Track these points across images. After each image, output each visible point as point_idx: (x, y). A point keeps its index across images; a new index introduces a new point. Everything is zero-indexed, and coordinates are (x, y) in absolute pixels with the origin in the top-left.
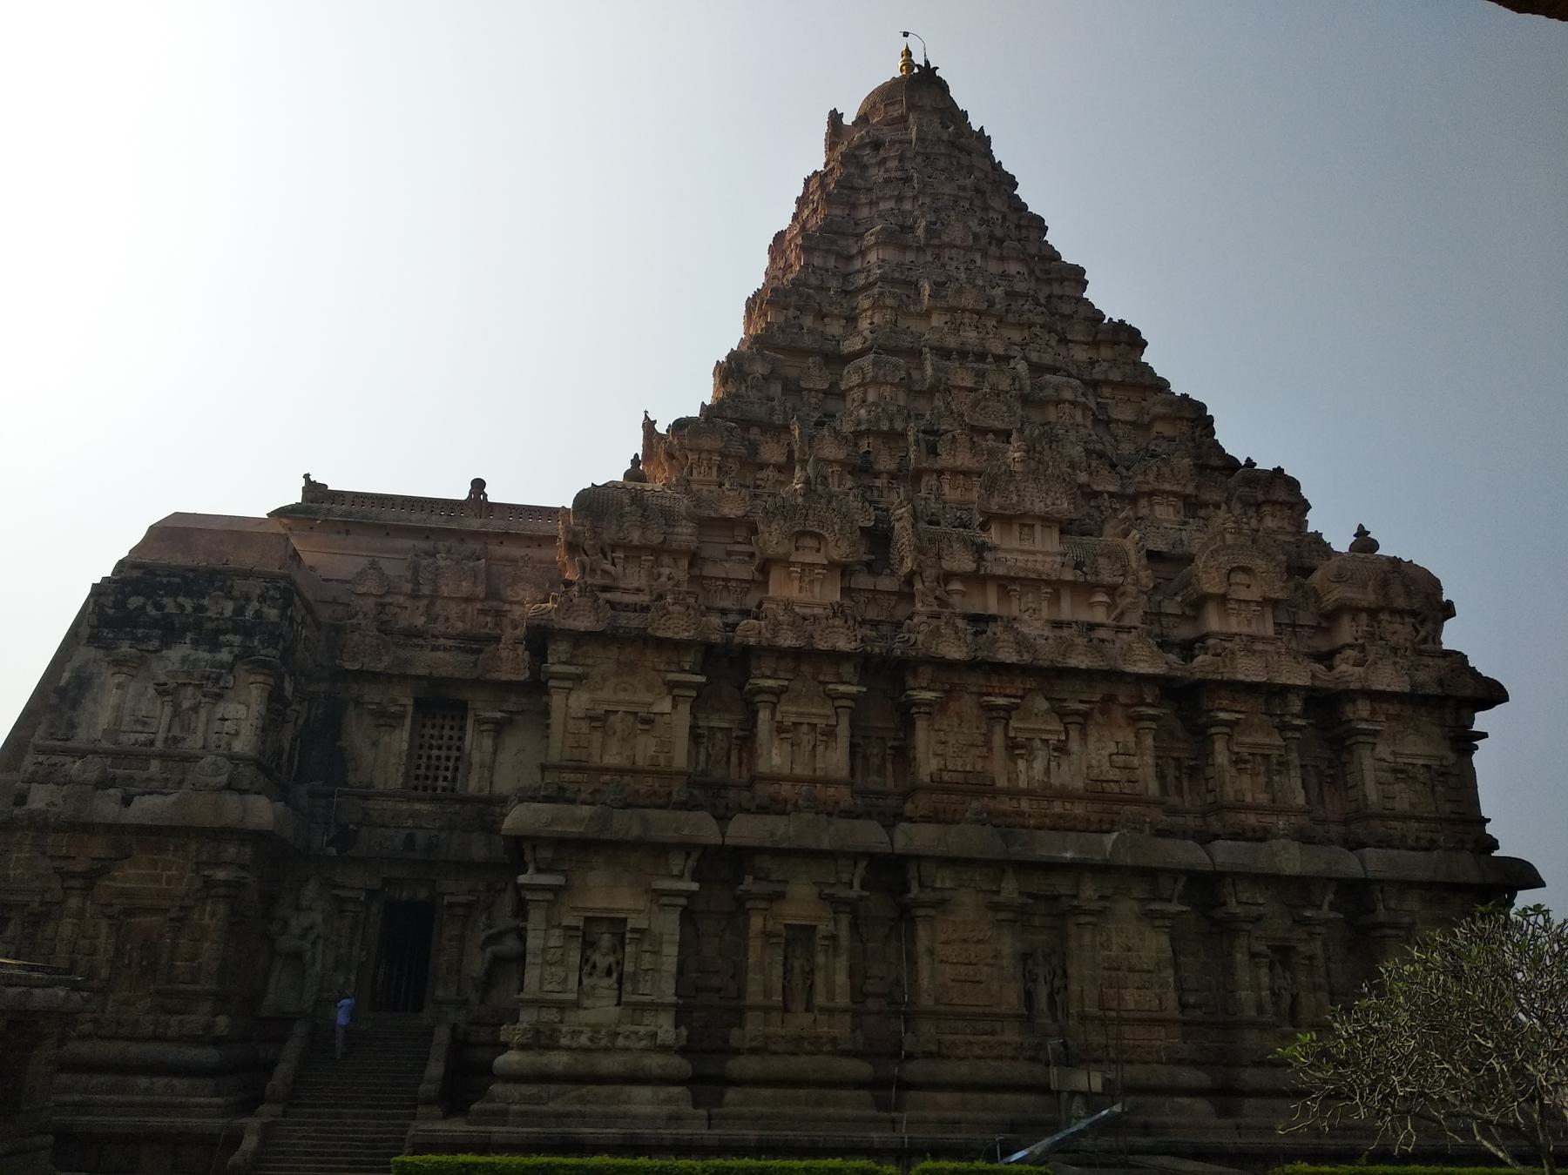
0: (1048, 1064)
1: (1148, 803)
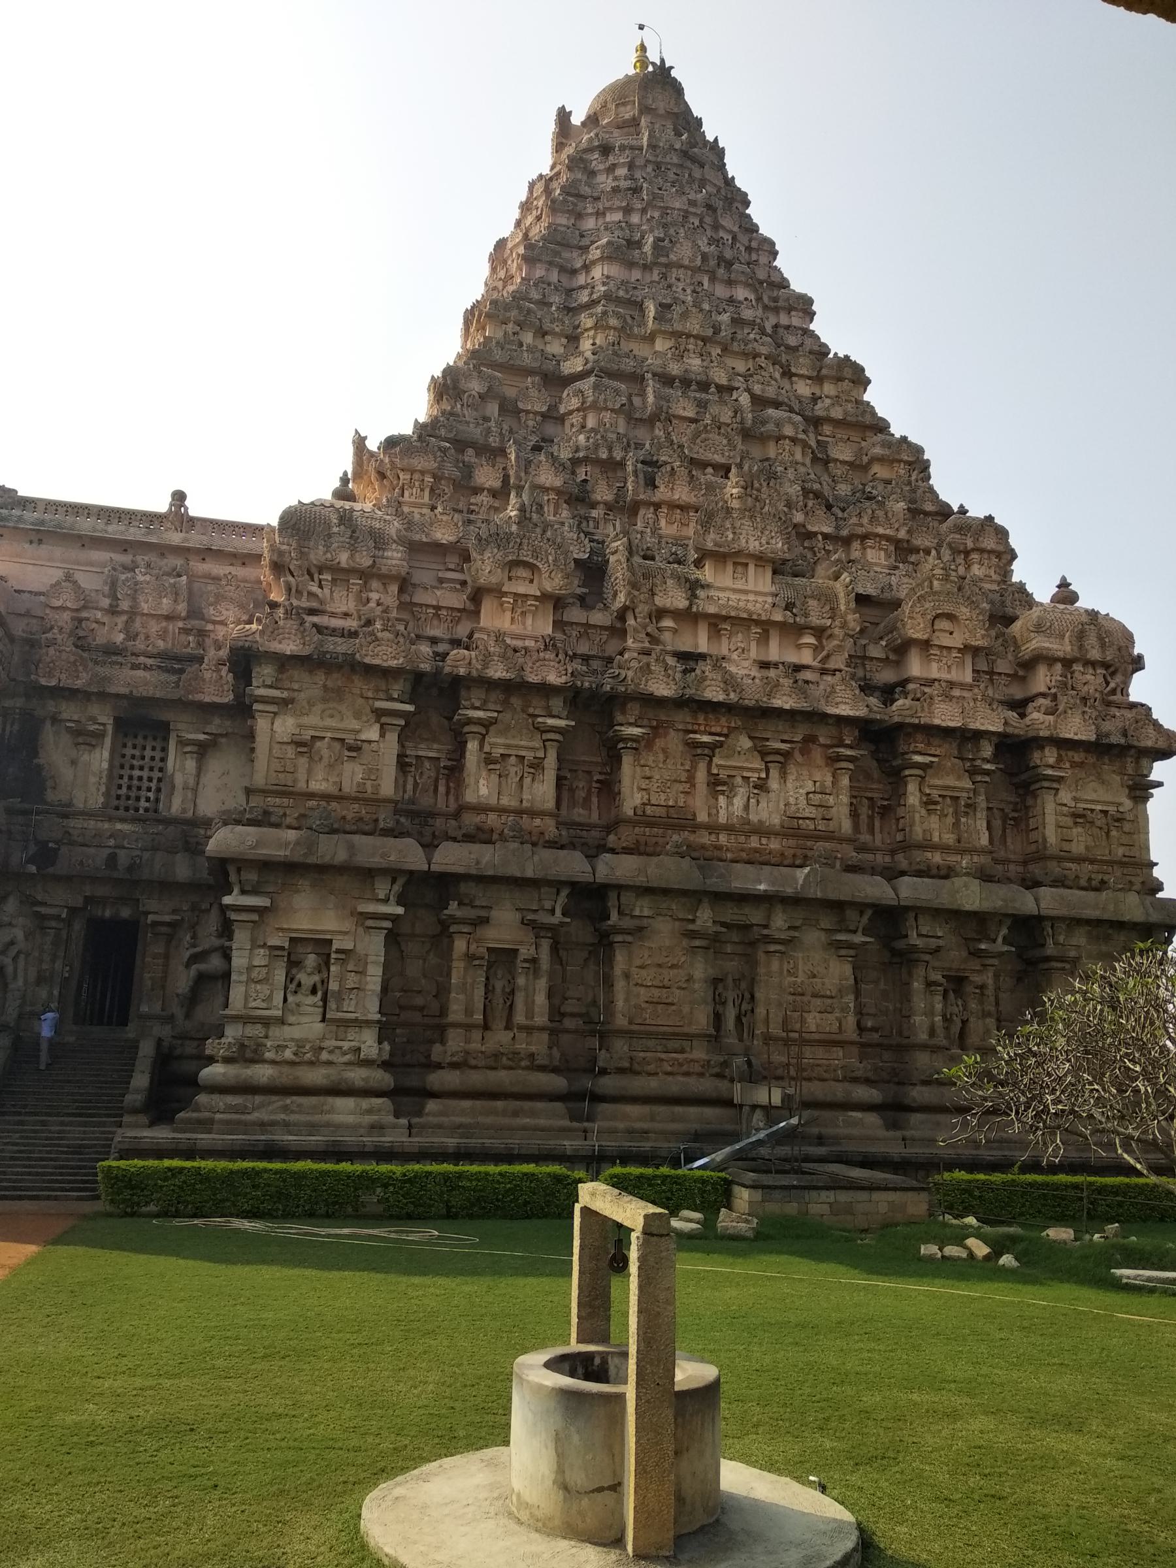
0: (732, 1081)
1: (841, 840)
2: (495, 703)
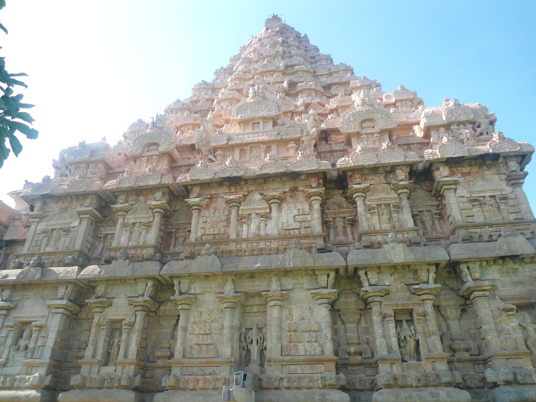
2: (132, 201)
